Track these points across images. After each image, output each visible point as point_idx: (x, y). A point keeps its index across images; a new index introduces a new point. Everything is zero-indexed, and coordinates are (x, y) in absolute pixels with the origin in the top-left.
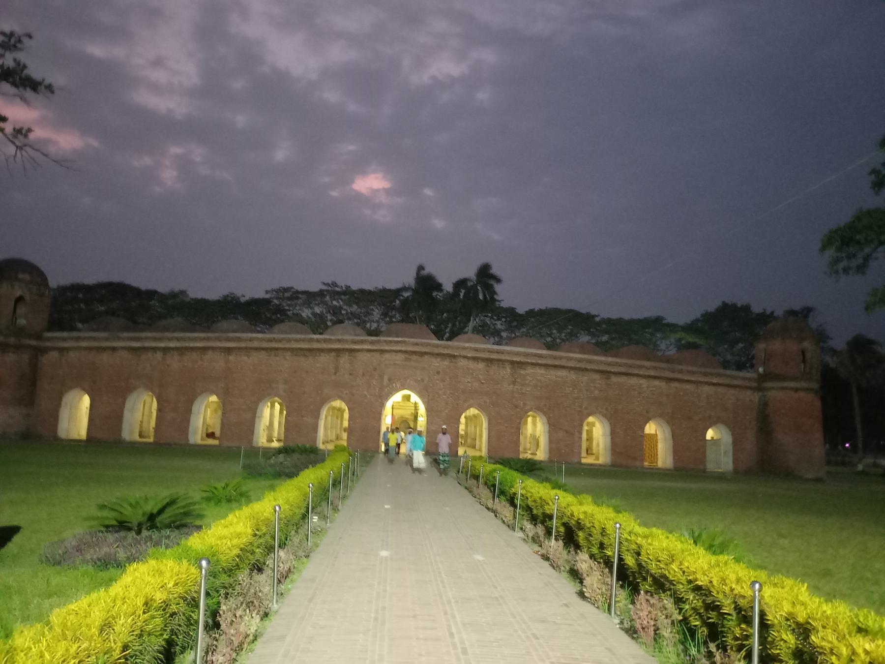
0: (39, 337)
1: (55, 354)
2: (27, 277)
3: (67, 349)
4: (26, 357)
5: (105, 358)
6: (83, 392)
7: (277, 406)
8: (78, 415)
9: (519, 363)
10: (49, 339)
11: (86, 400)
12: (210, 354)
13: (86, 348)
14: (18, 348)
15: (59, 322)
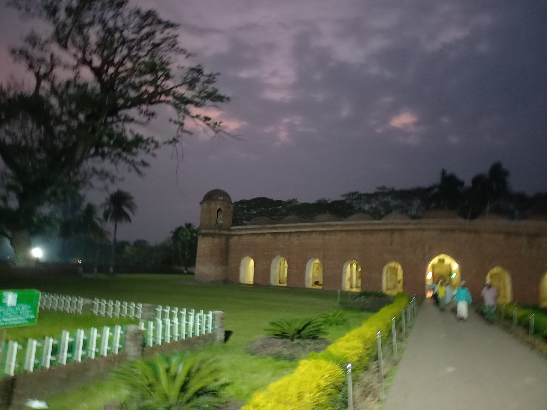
0: (229, 230)
1: (236, 238)
2: (222, 198)
3: (241, 235)
4: (223, 240)
6: (250, 258)
7: (354, 266)
8: (248, 271)
10: (234, 230)
11: (252, 262)
12: (314, 235)
13: (251, 234)
14: (220, 235)
15: (236, 221)
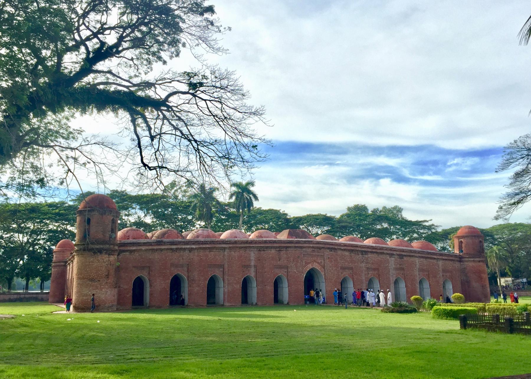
3: (134, 251)
5: (156, 256)
9: (365, 251)
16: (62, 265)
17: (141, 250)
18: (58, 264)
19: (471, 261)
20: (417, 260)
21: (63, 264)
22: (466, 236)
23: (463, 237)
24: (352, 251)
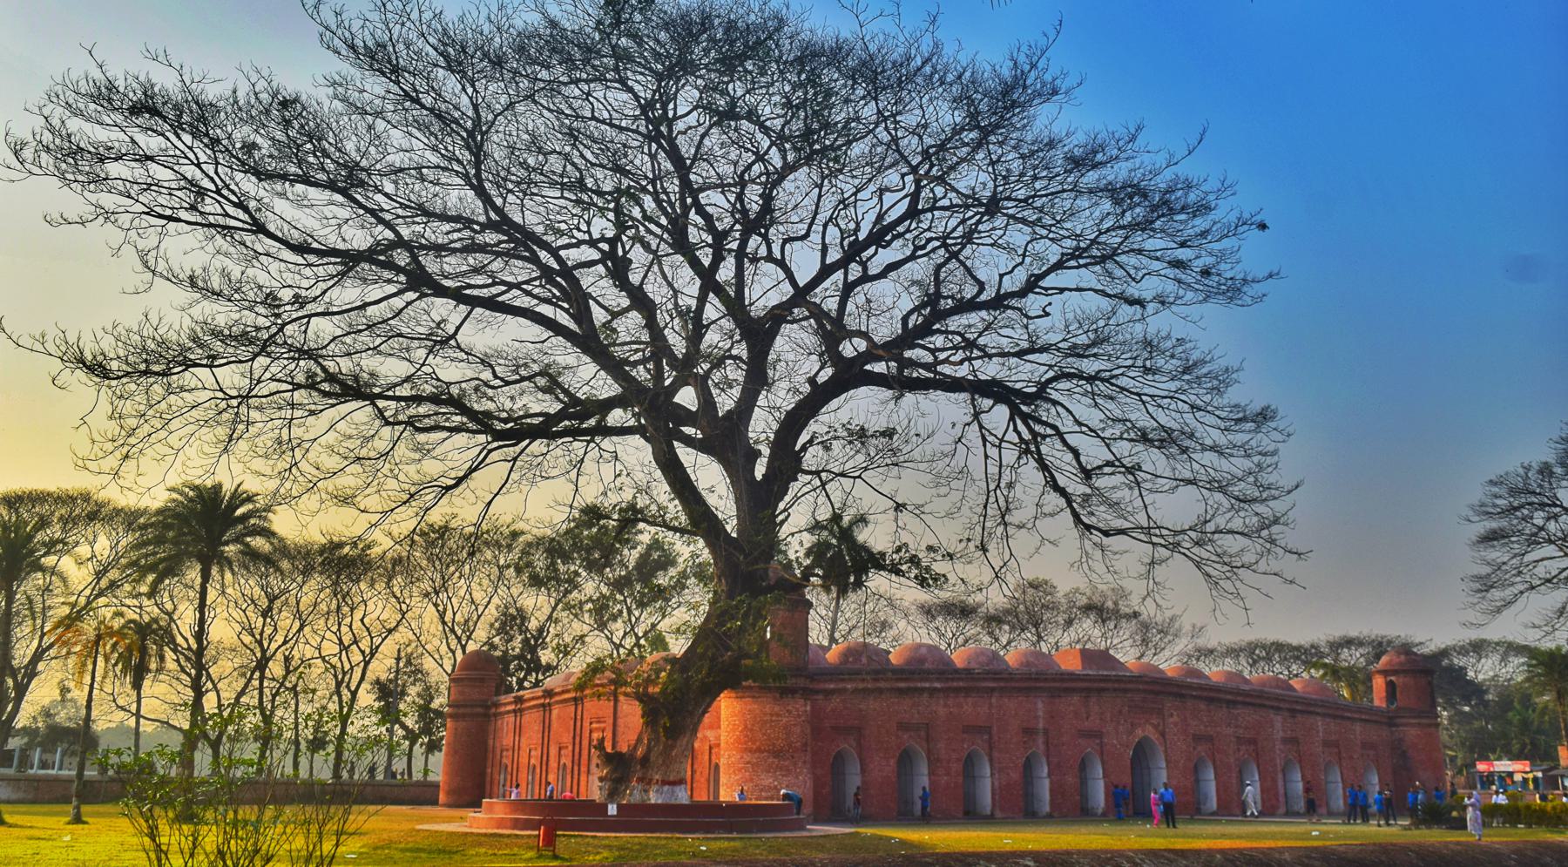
16: (478, 715)
17: (845, 690)
18: (468, 710)
19: (1412, 725)
20: (1320, 723)
21: (479, 710)
22: (1404, 671)
23: (1395, 672)
24: (1210, 700)
